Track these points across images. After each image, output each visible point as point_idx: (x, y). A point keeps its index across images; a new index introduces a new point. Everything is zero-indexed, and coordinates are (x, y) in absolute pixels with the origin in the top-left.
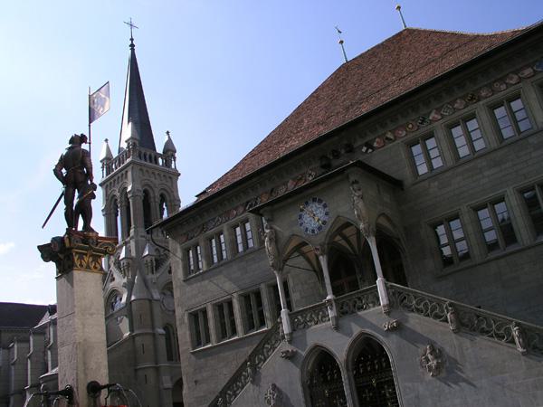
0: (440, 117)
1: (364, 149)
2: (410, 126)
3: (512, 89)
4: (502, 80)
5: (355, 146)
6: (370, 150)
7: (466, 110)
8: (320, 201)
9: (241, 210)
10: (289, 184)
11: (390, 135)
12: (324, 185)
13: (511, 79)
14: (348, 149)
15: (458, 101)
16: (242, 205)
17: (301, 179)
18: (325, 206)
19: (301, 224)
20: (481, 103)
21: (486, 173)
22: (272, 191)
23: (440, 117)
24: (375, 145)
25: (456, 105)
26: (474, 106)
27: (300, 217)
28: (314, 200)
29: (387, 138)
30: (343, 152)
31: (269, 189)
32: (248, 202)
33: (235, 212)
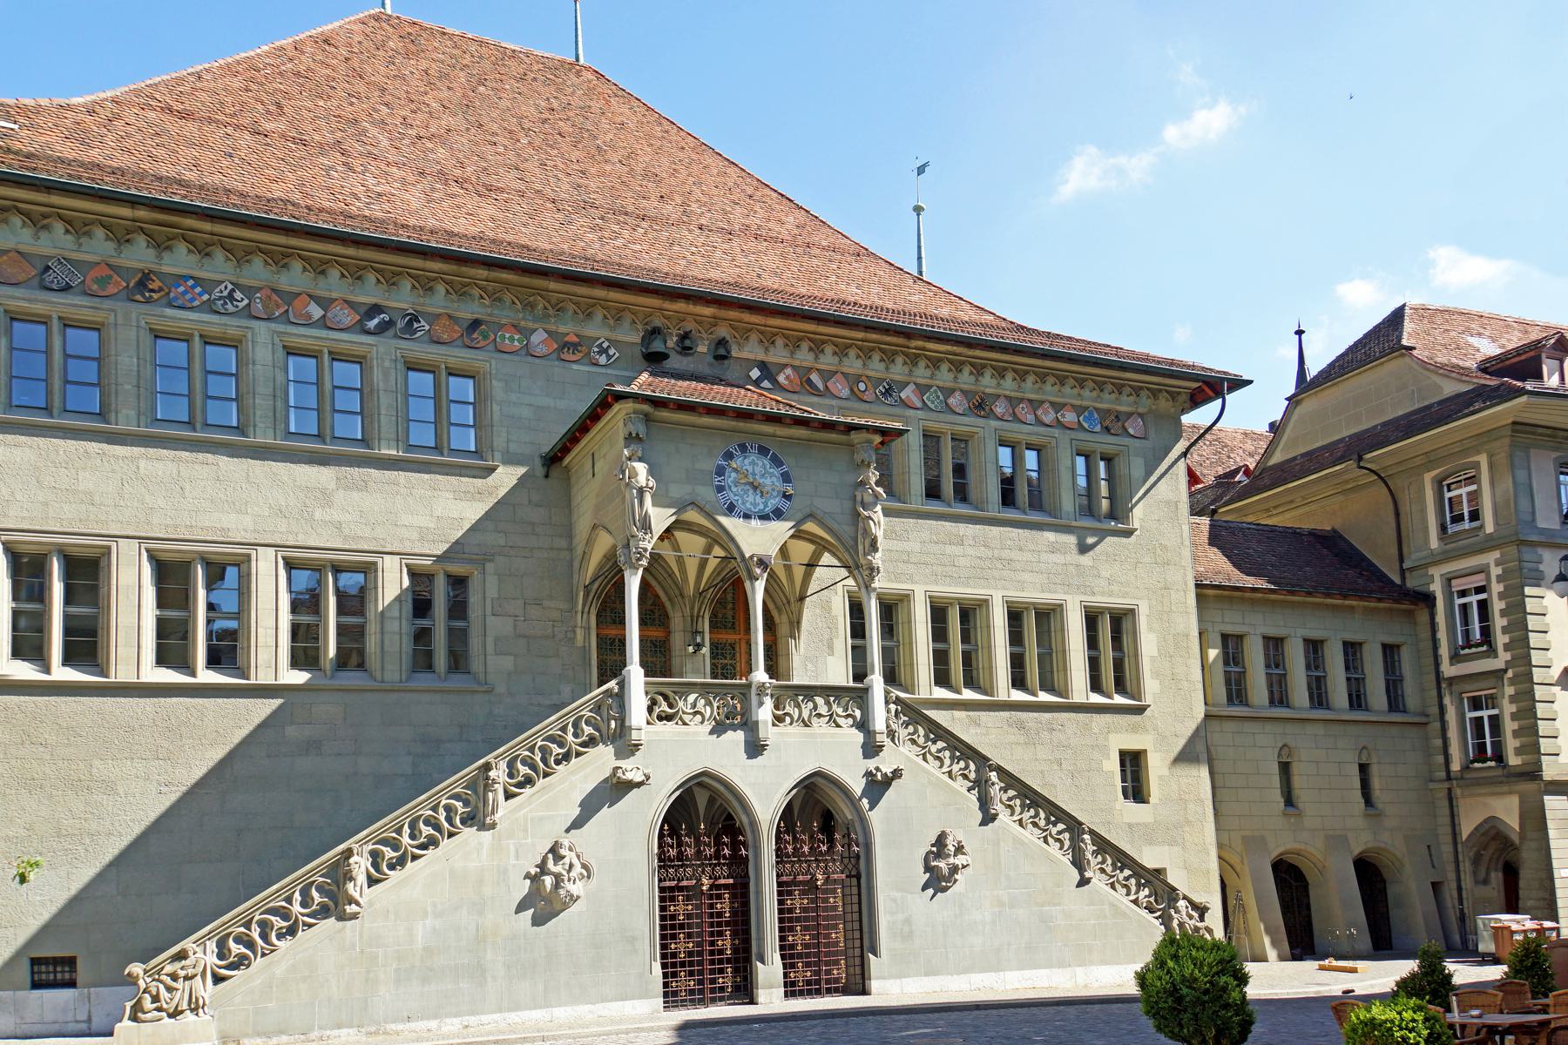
0: (919, 405)
1: (755, 374)
2: (862, 386)
3: (1042, 429)
4: (1035, 405)
5: (734, 354)
6: (766, 384)
7: (966, 420)
8: (776, 461)
9: (348, 317)
10: (538, 337)
11: (814, 377)
12: (801, 432)
13: (1046, 413)
14: (722, 352)
15: (957, 394)
16: (351, 305)
17: (575, 347)
18: (786, 478)
19: (720, 489)
20: (994, 423)
21: (970, 551)
22: (475, 324)
23: (919, 405)
24: (781, 378)
25: (951, 401)
26: (981, 422)
27: (720, 471)
28: (763, 451)
29: (809, 381)
30: (702, 348)
31: (469, 310)
32: (375, 310)
33: (316, 312)
